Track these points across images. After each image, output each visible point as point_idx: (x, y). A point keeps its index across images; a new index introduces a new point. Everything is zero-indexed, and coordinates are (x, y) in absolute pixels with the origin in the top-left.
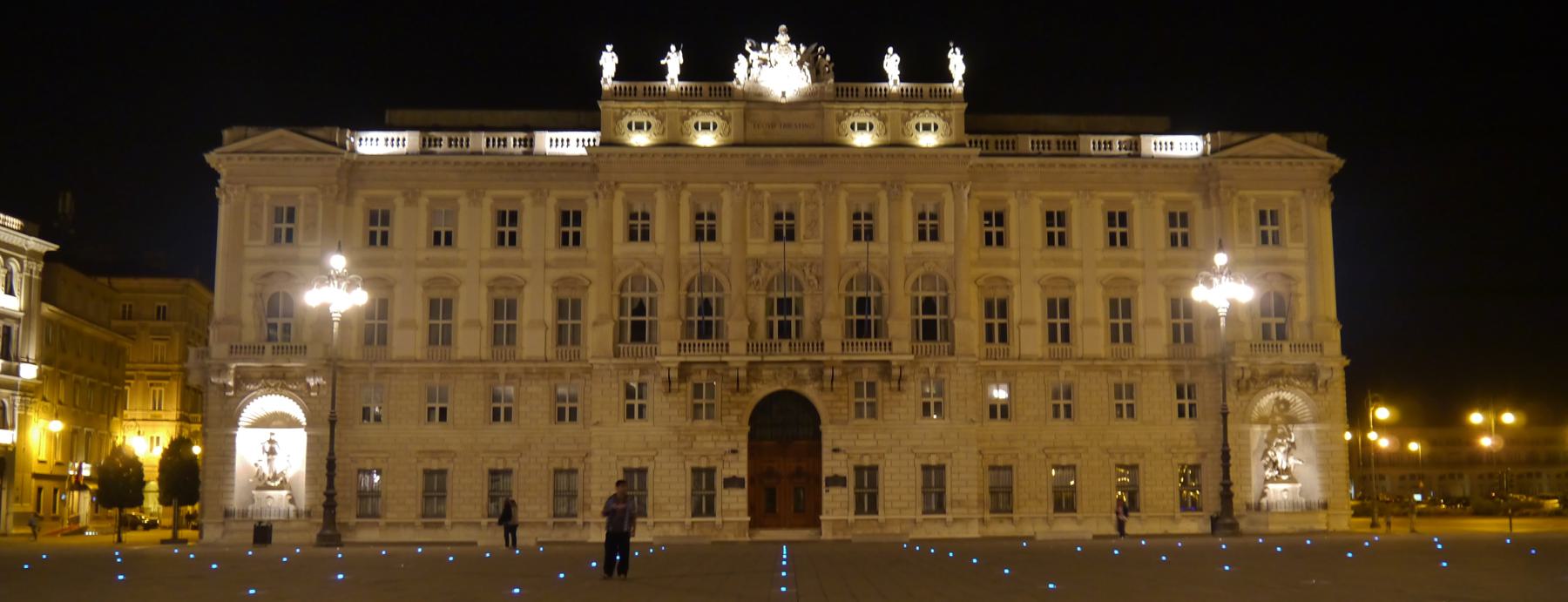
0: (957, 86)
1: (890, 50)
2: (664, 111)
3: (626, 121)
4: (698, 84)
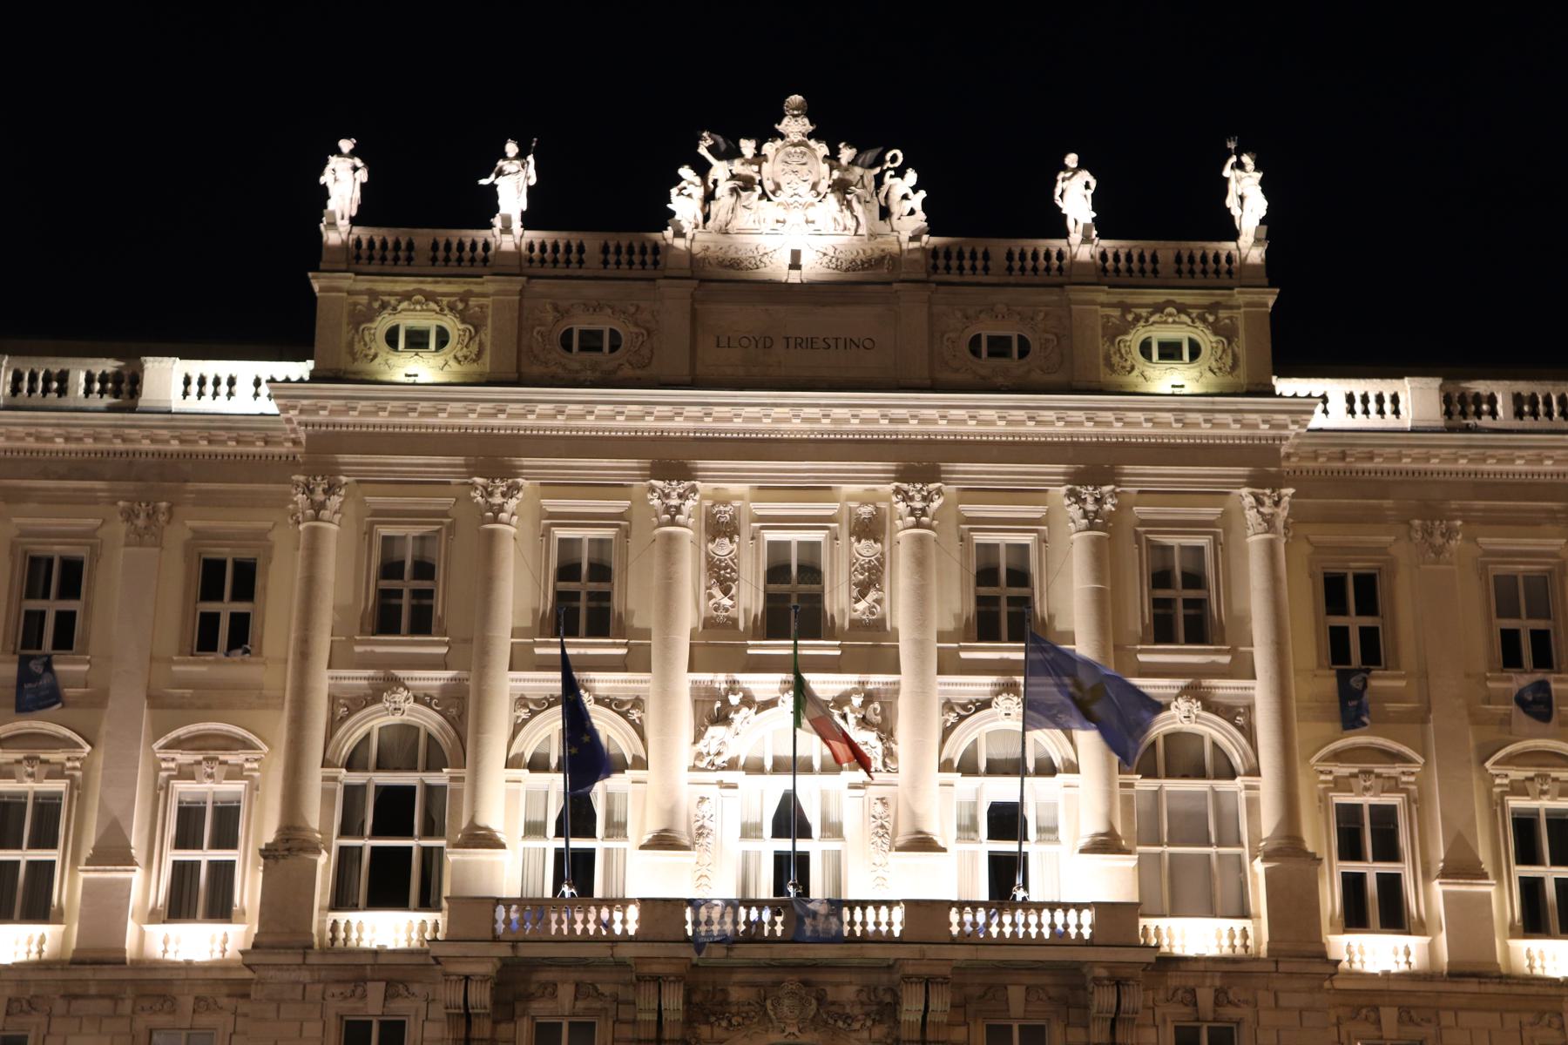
0: (1249, 247)
1: (1072, 160)
2: (483, 301)
3: (383, 323)
4: (574, 237)
